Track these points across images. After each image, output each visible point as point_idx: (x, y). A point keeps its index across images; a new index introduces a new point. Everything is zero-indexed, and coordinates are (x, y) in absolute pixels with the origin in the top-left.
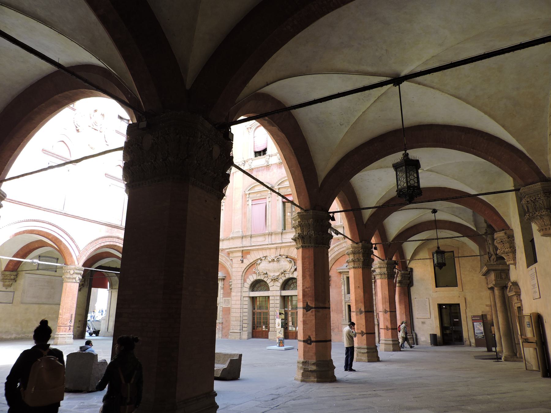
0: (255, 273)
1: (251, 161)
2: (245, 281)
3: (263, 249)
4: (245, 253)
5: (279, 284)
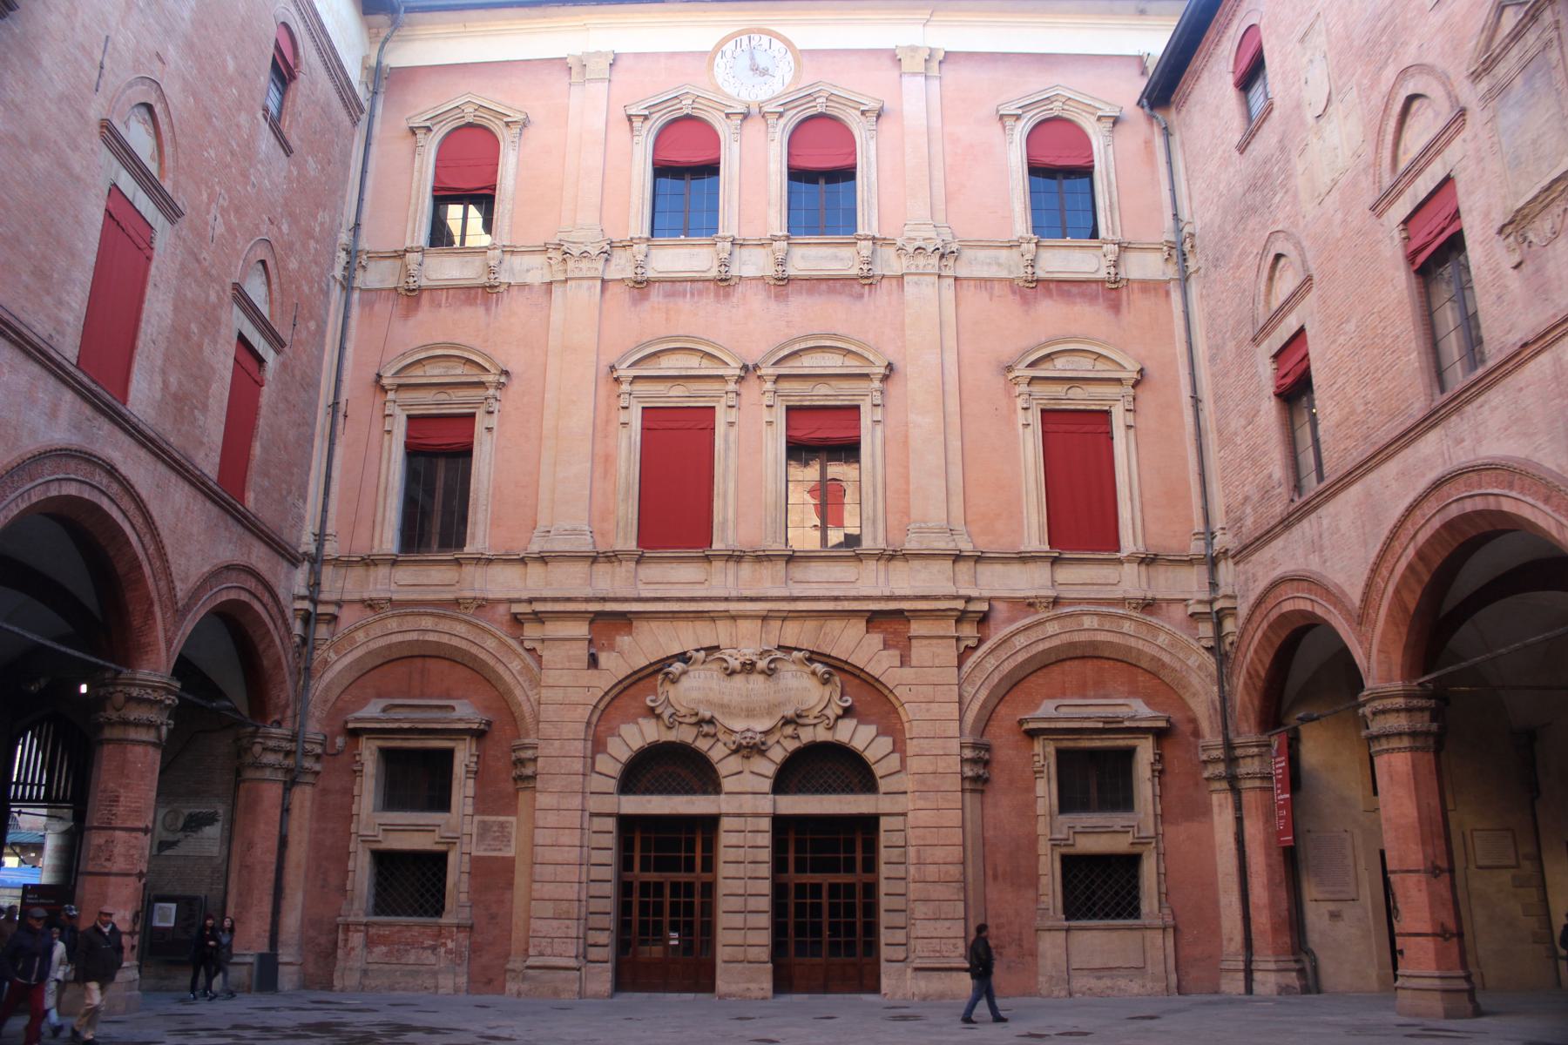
0: (652, 712)
1: (644, 247)
2: (598, 746)
3: (698, 615)
4: (610, 622)
5: (767, 768)
